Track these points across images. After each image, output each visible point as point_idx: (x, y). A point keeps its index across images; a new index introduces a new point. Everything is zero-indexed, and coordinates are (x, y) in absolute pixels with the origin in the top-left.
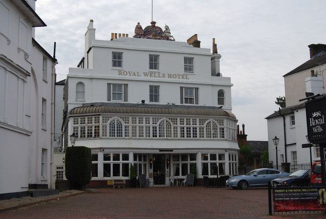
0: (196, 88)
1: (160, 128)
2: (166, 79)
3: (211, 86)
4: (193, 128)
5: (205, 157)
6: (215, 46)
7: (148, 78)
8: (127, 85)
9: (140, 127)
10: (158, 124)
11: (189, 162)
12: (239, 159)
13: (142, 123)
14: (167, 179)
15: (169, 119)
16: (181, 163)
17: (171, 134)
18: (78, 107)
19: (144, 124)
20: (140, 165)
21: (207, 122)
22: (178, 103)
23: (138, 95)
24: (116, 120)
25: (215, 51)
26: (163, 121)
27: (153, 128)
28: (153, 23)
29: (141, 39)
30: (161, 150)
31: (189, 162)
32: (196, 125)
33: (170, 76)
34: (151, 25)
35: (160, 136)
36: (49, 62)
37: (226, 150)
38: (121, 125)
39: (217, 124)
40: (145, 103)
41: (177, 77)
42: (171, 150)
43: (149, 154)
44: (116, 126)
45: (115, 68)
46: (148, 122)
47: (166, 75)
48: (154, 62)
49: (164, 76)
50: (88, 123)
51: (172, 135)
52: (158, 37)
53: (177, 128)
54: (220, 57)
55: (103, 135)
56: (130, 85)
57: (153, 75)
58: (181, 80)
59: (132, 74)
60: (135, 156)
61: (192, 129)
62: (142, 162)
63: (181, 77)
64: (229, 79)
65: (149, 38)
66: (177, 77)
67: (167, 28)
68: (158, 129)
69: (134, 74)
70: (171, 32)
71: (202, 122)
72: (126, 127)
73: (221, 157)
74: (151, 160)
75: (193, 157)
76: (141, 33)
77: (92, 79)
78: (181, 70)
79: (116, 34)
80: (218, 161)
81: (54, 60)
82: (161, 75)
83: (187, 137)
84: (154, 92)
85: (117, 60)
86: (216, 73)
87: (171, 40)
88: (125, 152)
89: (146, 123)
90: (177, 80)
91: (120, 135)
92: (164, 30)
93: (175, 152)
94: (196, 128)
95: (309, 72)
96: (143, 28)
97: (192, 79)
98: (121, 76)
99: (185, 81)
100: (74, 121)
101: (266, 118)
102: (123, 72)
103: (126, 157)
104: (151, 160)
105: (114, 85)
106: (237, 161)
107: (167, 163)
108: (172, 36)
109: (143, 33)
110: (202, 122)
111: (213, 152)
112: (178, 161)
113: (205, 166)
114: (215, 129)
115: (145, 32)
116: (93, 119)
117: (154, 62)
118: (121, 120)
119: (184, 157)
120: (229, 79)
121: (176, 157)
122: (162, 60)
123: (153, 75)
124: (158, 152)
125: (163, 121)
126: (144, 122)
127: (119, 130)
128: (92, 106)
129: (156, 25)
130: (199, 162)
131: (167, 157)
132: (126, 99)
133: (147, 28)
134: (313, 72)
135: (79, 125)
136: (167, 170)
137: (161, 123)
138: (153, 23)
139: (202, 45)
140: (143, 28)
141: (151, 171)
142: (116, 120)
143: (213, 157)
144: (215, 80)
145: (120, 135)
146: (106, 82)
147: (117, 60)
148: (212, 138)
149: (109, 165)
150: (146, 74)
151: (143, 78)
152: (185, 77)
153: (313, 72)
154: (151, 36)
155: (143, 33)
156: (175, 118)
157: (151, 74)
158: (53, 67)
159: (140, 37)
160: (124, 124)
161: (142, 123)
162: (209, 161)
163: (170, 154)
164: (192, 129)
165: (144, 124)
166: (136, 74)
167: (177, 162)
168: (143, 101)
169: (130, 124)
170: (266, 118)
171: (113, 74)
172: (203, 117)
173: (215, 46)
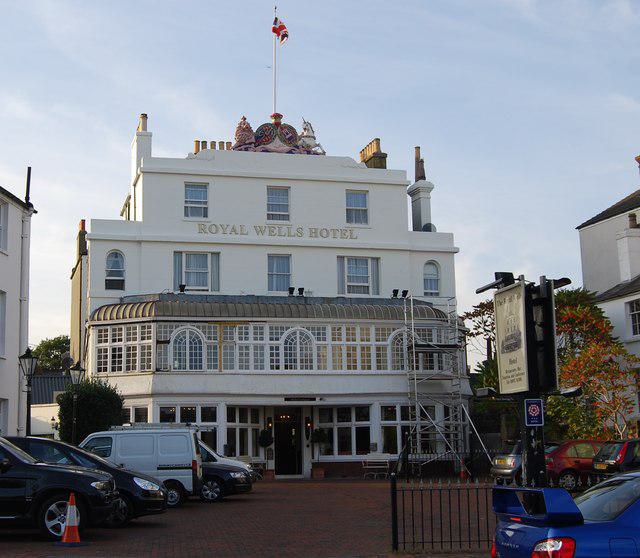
0: (373, 259)
1: (286, 349)
2: (306, 240)
4: (363, 349)
5: (388, 412)
6: (419, 163)
7: (266, 238)
8: (218, 254)
10: (281, 342)
11: (354, 424)
14: (307, 467)
15: (308, 329)
17: (201, 361)
18: (109, 306)
20: (243, 432)
23: (243, 276)
24: (188, 332)
25: (420, 175)
26: (295, 333)
27: (272, 348)
31: (354, 424)
33: (314, 233)
35: (286, 367)
36: (14, 211)
41: (331, 233)
43: (265, 407)
45: (190, 218)
47: (306, 232)
48: (278, 204)
54: (430, 188)
56: (224, 252)
57: (276, 231)
58: (340, 242)
59: (229, 229)
60: (231, 411)
61: (359, 349)
62: (249, 426)
63: (338, 234)
64: (450, 237)
65: (267, 151)
66: (331, 233)
67: (307, 126)
68: (282, 351)
70: (316, 135)
71: (382, 334)
75: (363, 412)
76: (254, 139)
77: (139, 242)
79: (204, 143)
80: (417, 423)
81: (27, 206)
82: (294, 231)
84: (279, 265)
85: (196, 199)
86: (423, 226)
87: (316, 153)
88: (208, 402)
89: (255, 339)
90: (330, 241)
91: (196, 364)
92: (300, 131)
93: (317, 402)
95: (623, 219)
97: (364, 238)
99: (348, 243)
100: (100, 336)
104: (270, 421)
105: (189, 254)
108: (318, 145)
112: (332, 421)
113: (389, 433)
116: (138, 330)
117: (278, 204)
119: (344, 412)
120: (450, 237)
121: (326, 412)
122: (297, 200)
123: (276, 231)
124: (281, 402)
125: (295, 333)
126: (251, 335)
129: (283, 121)
130: (376, 425)
131: (306, 414)
132: (217, 285)
133: (264, 128)
134: (633, 217)
135: (108, 345)
137: (288, 337)
138: (277, 116)
139: (390, 163)
142: (188, 332)
144: (423, 240)
147: (196, 199)
148: (237, 370)
150: (259, 230)
151: (253, 238)
152: (348, 234)
153: (633, 217)
158: (25, 223)
159: (246, 149)
162: (398, 422)
163: (312, 407)
164: (359, 349)
166: (238, 230)
167: (329, 425)
171: (189, 232)
172: (279, 321)
173: (419, 163)
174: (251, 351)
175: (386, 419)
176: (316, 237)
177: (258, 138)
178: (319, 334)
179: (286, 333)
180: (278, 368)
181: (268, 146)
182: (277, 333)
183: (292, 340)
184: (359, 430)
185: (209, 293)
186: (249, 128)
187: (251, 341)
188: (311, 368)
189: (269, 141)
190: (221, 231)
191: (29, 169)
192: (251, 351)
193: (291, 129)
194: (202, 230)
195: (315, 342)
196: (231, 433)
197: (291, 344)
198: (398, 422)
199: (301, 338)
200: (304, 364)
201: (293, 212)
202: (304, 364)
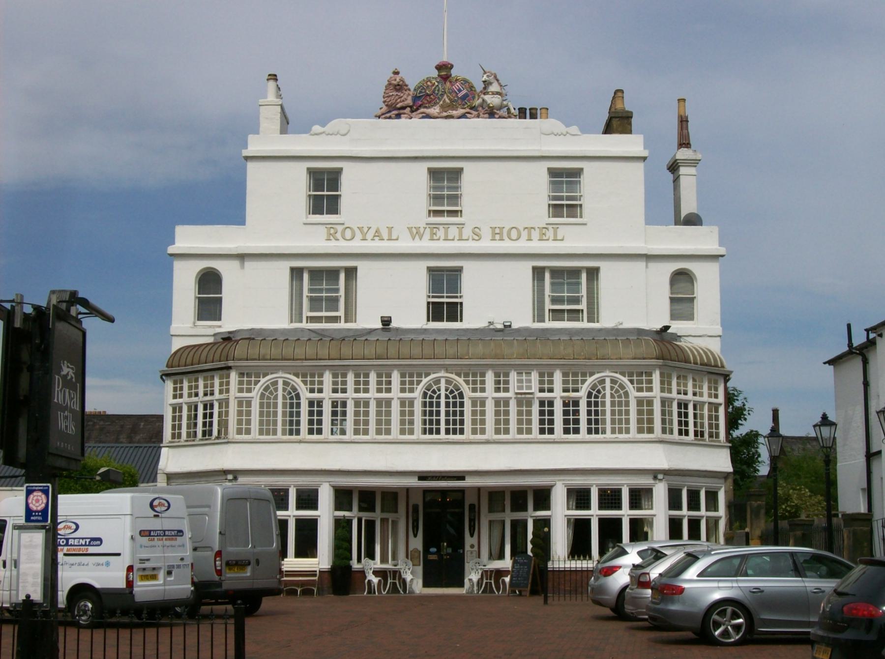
3: (641, 265)
5: (580, 498)
6: (683, 121)
11: (531, 516)
12: (729, 506)
13: (366, 391)
14: (473, 576)
16: (508, 516)
19: (373, 394)
20: (371, 524)
22: (523, 319)
28: (444, 69)
29: (403, 121)
30: (423, 476)
32: (551, 390)
33: (497, 234)
34: (435, 73)
37: (655, 474)
39: (630, 387)
40: (394, 324)
41: (525, 234)
42: (460, 476)
44: (443, 401)
46: (385, 385)
47: (486, 233)
49: (477, 234)
50: (205, 394)
51: (468, 426)
52: (461, 111)
53: (483, 404)
55: (239, 432)
56: (363, 267)
58: (536, 246)
59: (371, 233)
60: (343, 497)
63: (535, 235)
65: (428, 116)
66: (525, 234)
69: (378, 235)
72: (311, 403)
73: (639, 497)
74: (416, 508)
75: (543, 497)
78: (540, 214)
82: (467, 232)
83: (542, 431)
88: (306, 482)
89: (379, 390)
92: (479, 87)
93: (469, 482)
94: (551, 403)
98: (333, 243)
99: (549, 247)
101: (830, 362)
102: (340, 228)
103: (308, 499)
106: (722, 511)
107: (472, 521)
109: (409, 101)
118: (298, 382)
121: (496, 497)
123: (441, 233)
124: (413, 482)
125: (437, 381)
126: (373, 385)
128: (225, 339)
131: (469, 500)
136: (469, 541)
140: (412, 87)
141: (417, 543)
143: (610, 499)
146: (285, 267)
149: (618, 522)
150: (416, 233)
151: (406, 245)
152: (550, 234)
154: (435, 110)
155: (409, 101)
157: (434, 227)
159: (398, 116)
160: (305, 395)
161: (366, 391)
165: (373, 394)
166: (386, 236)
168: (386, 322)
170: (830, 362)
173: (683, 121)
175: (578, 507)
176: (501, 239)
177: (415, 98)
178: (474, 382)
179: (425, 381)
180: (320, 432)
181: (431, 111)
182: (411, 383)
183: (434, 392)
184: (300, 522)
185: (342, 325)
186: (400, 87)
187: (373, 394)
188: (462, 432)
189: (432, 103)
190: (359, 235)
193: (465, 81)
194: (331, 236)
195: (633, 394)
196: (342, 527)
197: (431, 397)
198: (595, 513)
199: (612, 388)
201: (466, 204)
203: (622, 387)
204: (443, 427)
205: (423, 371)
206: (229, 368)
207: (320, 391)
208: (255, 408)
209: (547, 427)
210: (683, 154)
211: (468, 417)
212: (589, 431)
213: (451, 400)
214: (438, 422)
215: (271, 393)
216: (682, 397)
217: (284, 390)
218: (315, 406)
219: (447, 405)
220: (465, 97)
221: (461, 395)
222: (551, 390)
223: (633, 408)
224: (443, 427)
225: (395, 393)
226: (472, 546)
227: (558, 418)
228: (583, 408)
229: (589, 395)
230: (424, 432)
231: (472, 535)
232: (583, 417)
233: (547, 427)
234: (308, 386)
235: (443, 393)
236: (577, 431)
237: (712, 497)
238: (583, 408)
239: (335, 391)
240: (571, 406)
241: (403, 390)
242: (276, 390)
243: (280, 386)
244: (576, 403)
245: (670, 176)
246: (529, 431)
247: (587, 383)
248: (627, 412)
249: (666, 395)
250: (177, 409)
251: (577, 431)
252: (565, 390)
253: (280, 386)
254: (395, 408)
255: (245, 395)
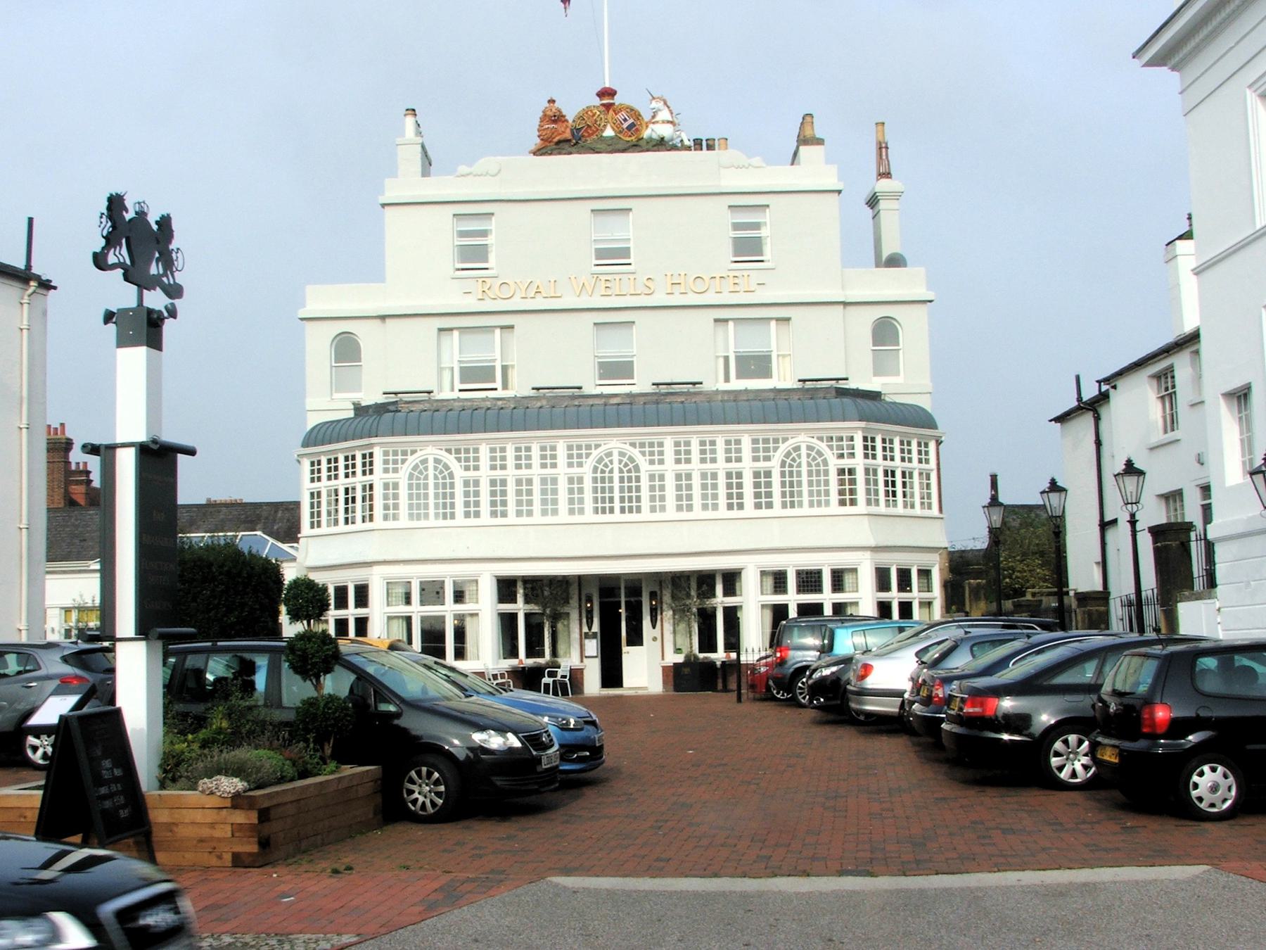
4: (729, 475)
6: (882, 147)
9: (544, 481)
12: (948, 586)
21: (783, 448)
27: (571, 481)
34: (597, 102)
38: (451, 476)
51: (645, 503)
60: (506, 588)
71: (763, 450)
75: (731, 580)
77: (383, 318)
89: (544, 466)
96: (570, 115)
109: (568, 135)
110: (763, 450)
111: (809, 561)
114: (818, 471)
115: (576, 131)
118: (450, 459)
119: (705, 581)
121: (678, 581)
127: (418, 497)
129: (617, 100)
138: (607, 93)
140: (570, 115)
143: (809, 581)
145: (631, 505)
156: (655, 439)
169: (485, 474)
173: (882, 147)
174: (536, 487)
180: (477, 514)
185: (500, 393)
186: (558, 118)
187: (536, 472)
188: (639, 510)
191: (31, 221)
192: (536, 487)
197: (602, 472)
200: (626, 504)
202: (626, 504)
203: (820, 454)
204: (617, 505)
205: (593, 442)
206: (372, 445)
207: (476, 468)
208: (403, 492)
209: (735, 501)
210: (884, 185)
211: (645, 494)
212: (784, 506)
213: (626, 475)
214: (611, 500)
215: (421, 473)
216: (888, 463)
217: (436, 468)
218: (472, 486)
219: (622, 480)
220: (632, 125)
221: (637, 469)
222: (739, 460)
223: (833, 478)
224: (617, 505)
225: (562, 471)
226: (655, 639)
227: (748, 490)
228: (776, 479)
229: (783, 464)
230: (596, 511)
231: (654, 627)
232: (776, 489)
233: (735, 501)
234: (463, 464)
235: (616, 466)
236: (770, 505)
237: (925, 574)
238: (776, 479)
239: (493, 468)
240: (761, 478)
241: (570, 465)
242: (426, 469)
243: (431, 464)
244: (768, 474)
245: (869, 212)
246: (715, 507)
247: (779, 451)
248: (827, 483)
249: (870, 461)
250: (315, 495)
251: (770, 505)
252: (756, 459)
253: (431, 464)
254: (563, 486)
255: (391, 475)
